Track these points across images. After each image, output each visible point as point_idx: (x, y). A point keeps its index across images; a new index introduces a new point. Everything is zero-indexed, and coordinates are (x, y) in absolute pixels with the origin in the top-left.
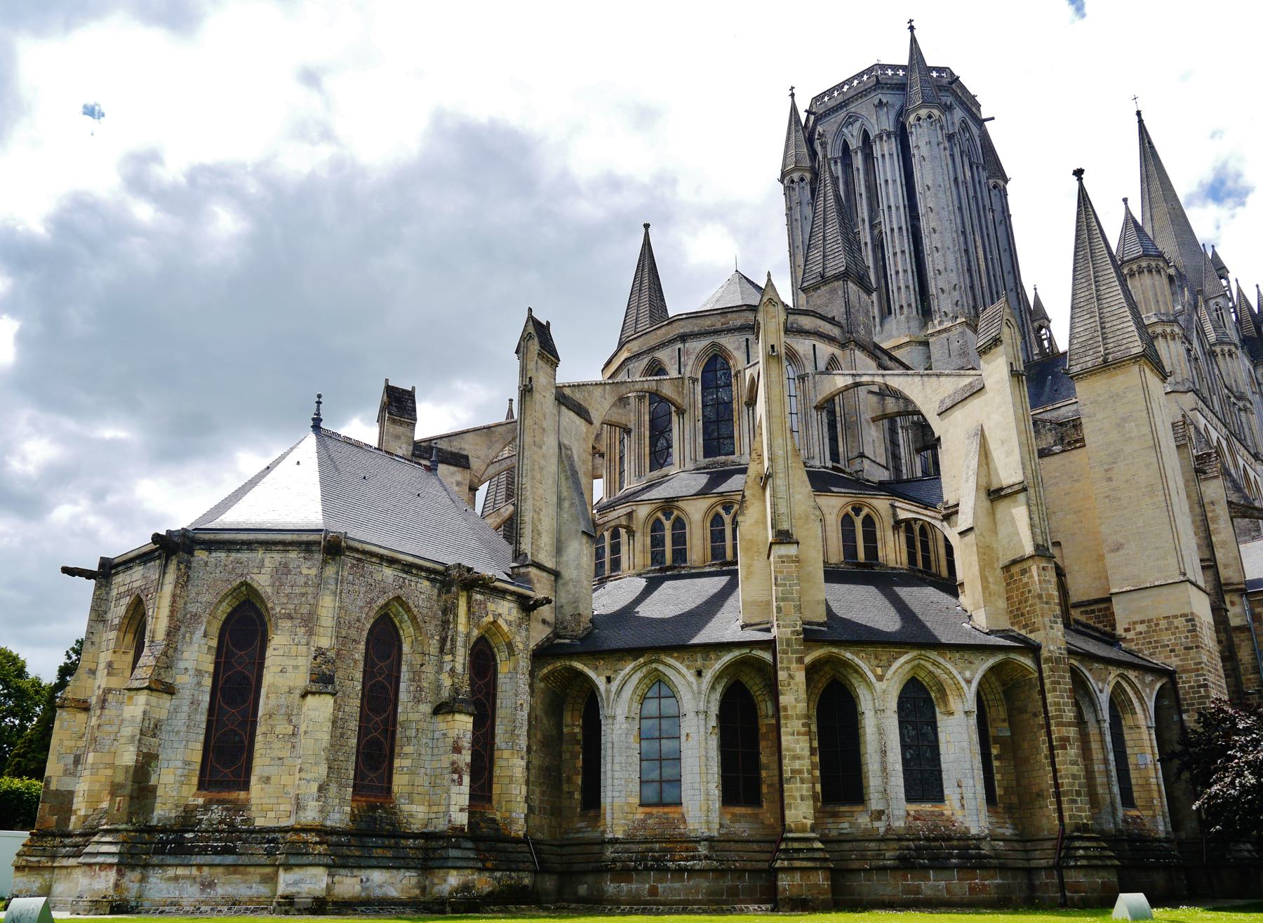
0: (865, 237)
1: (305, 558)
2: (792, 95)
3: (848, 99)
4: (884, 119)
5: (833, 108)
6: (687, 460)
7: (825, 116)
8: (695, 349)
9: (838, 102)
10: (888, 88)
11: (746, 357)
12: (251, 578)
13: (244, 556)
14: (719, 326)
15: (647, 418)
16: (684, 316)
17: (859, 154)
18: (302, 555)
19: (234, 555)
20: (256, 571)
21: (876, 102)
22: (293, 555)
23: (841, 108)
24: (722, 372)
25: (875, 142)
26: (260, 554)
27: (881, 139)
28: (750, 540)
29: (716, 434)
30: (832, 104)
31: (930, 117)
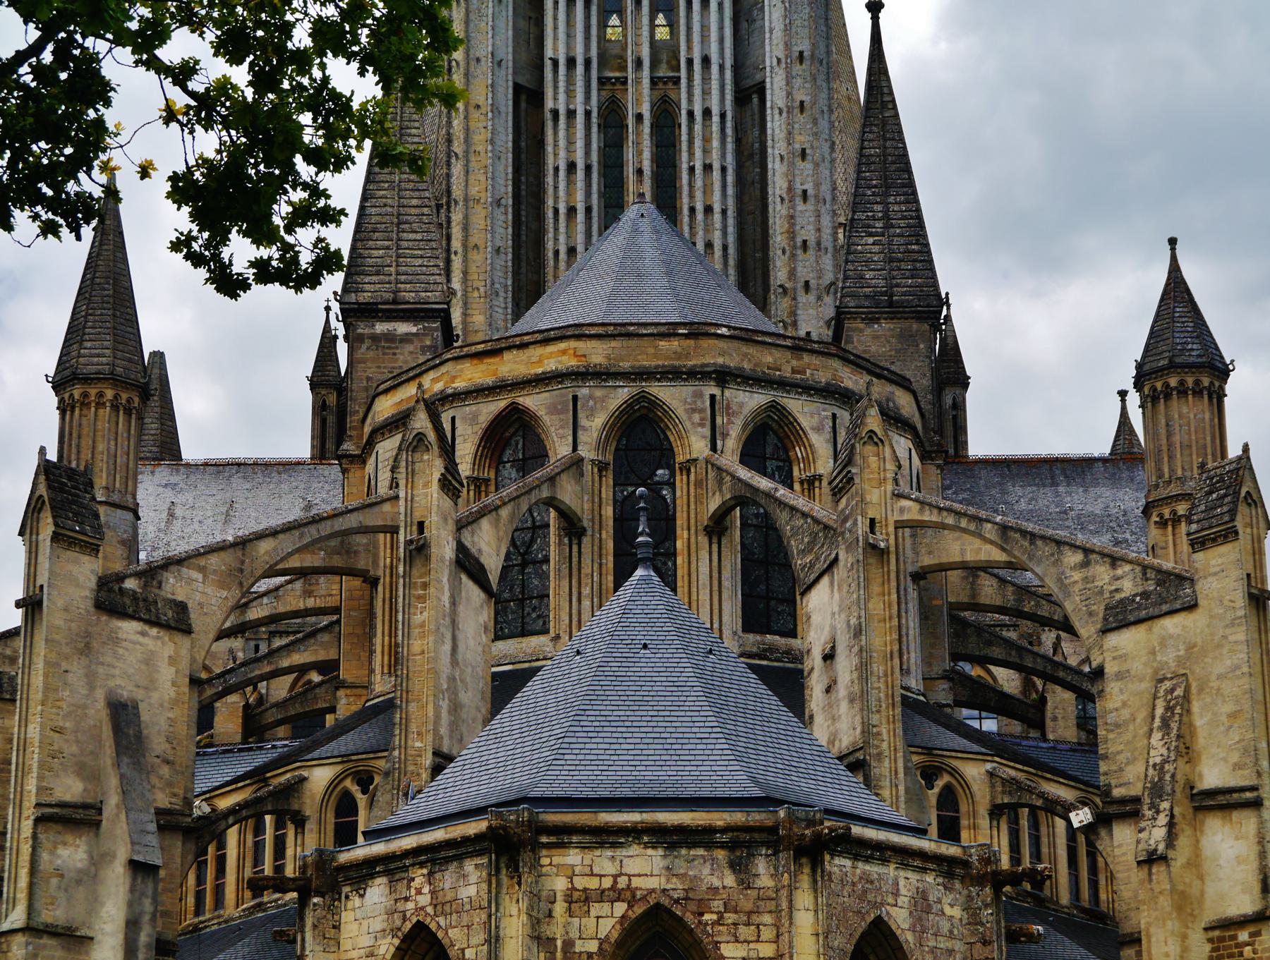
0: (638, 102)
1: (946, 888)
6: (727, 633)
8: (741, 405)
12: (888, 913)
13: (874, 869)
14: (787, 373)
15: (609, 511)
16: (724, 331)
18: (940, 880)
19: (860, 864)
20: (890, 900)
22: (930, 878)
26: (891, 871)
28: (1183, 892)
29: (763, 587)
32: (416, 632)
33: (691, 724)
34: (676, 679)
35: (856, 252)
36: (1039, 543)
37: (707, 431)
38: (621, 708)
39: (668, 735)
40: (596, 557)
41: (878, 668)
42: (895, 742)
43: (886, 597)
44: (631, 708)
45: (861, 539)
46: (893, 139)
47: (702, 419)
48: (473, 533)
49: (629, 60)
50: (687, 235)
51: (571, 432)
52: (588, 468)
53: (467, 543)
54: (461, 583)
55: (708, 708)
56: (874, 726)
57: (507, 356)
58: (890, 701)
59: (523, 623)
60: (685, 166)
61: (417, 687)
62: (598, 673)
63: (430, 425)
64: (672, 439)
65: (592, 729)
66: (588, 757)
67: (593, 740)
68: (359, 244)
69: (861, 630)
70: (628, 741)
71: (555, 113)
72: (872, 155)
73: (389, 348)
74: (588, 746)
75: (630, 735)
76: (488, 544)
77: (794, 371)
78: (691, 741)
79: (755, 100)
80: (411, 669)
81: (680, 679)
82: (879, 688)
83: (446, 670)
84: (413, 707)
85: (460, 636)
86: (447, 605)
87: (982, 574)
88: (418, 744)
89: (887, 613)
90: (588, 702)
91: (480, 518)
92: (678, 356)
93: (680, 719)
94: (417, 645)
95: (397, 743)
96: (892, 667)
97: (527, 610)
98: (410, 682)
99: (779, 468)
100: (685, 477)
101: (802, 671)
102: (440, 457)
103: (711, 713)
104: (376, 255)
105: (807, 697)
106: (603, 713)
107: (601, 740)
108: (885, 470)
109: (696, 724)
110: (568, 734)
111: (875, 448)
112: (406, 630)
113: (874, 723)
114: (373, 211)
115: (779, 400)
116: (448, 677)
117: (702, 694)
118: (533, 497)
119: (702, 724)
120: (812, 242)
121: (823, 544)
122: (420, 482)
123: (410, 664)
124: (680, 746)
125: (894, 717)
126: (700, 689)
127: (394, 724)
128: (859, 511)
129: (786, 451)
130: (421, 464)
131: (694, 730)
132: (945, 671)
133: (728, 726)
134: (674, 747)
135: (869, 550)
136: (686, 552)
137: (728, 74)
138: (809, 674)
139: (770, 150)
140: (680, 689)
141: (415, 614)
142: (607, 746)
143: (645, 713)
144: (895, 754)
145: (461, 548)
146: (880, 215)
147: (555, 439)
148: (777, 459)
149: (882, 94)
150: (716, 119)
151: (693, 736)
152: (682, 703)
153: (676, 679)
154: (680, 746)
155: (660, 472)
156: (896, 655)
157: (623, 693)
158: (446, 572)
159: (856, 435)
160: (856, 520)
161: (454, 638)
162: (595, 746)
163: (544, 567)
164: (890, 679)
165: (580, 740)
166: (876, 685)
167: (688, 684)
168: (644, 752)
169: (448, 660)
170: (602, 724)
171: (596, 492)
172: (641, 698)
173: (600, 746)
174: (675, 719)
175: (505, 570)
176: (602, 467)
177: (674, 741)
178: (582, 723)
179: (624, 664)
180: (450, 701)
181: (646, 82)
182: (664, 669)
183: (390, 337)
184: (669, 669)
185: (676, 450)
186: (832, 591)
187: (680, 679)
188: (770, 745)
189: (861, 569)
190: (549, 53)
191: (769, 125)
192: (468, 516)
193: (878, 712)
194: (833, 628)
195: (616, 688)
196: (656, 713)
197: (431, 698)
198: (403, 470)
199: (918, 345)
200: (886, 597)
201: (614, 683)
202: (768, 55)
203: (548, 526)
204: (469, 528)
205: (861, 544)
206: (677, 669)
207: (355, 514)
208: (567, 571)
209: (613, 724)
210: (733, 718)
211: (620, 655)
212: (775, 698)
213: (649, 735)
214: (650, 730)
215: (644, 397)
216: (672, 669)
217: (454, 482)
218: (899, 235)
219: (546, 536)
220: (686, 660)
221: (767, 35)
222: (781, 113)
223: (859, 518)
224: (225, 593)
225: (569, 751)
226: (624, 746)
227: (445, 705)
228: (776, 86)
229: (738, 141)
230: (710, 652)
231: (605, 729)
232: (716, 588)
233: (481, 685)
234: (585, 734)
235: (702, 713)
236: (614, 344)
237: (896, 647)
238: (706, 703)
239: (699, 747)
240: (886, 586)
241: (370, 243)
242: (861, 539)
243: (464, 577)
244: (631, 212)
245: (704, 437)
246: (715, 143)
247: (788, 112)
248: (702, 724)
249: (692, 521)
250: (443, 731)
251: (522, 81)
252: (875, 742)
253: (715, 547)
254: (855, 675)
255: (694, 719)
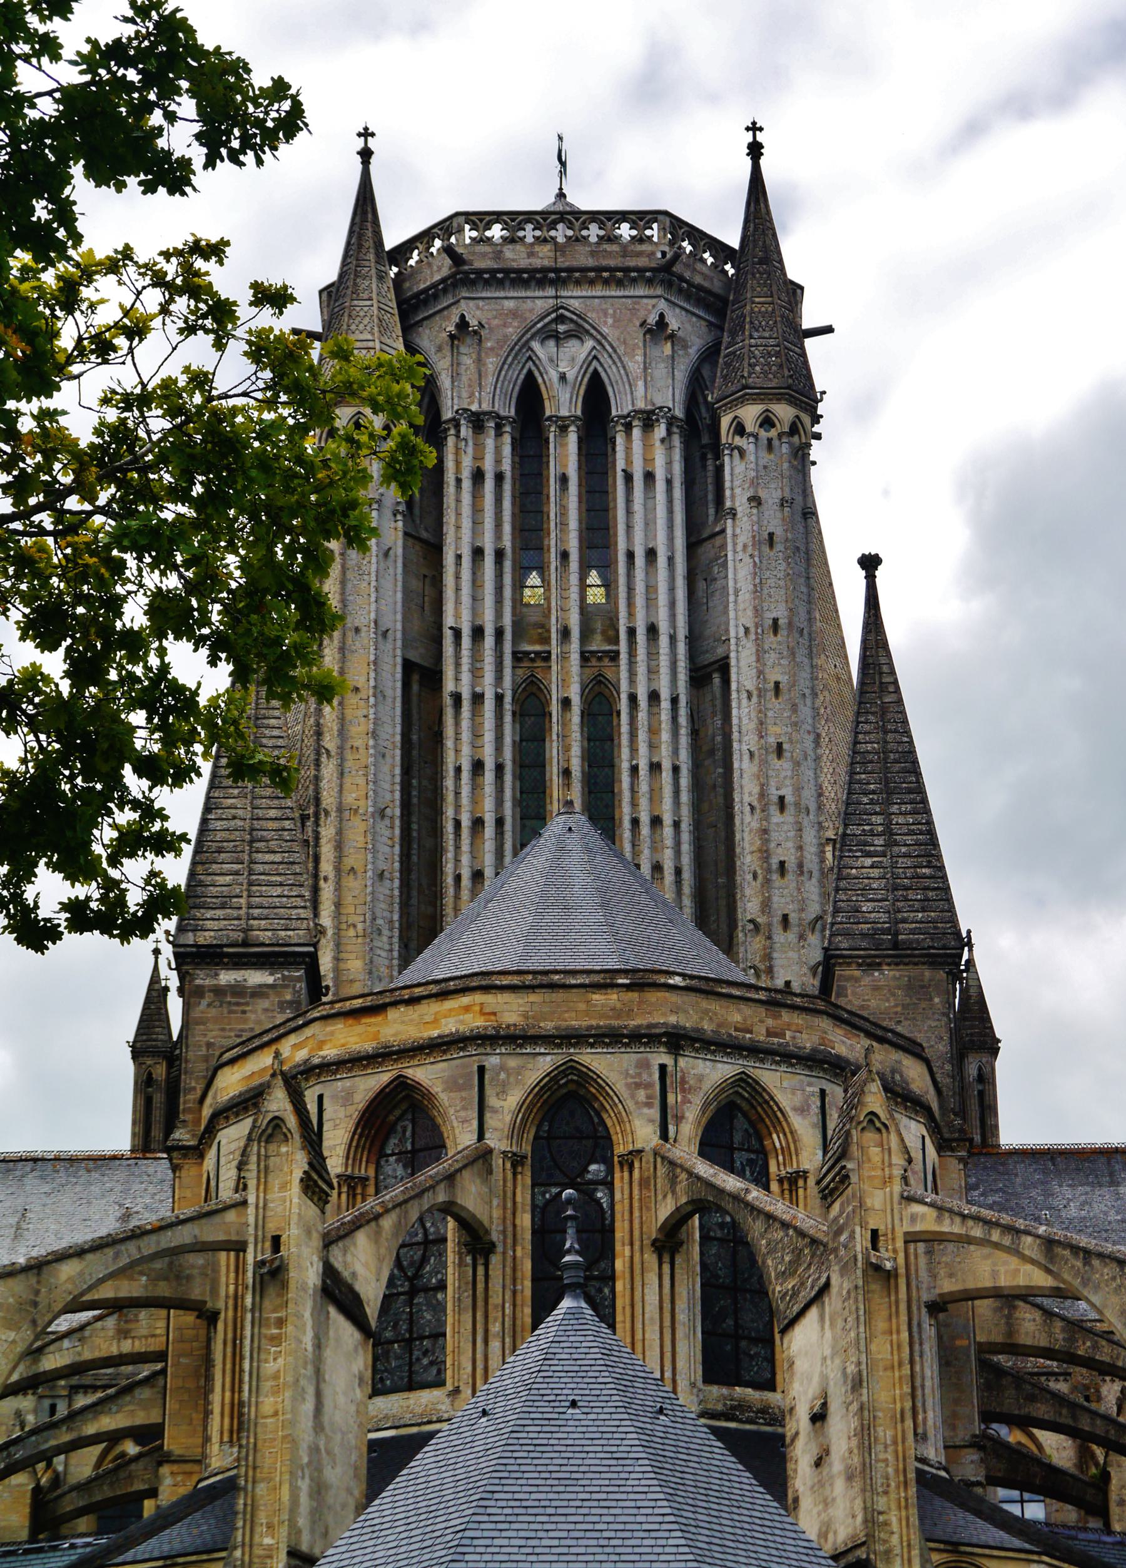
0: (564, 683)
2: (366, 154)
3: (570, 270)
4: (660, 371)
5: (520, 271)
6: (682, 1384)
7: (487, 283)
8: (700, 1078)
9: (537, 263)
10: (680, 291)
11: (820, 1136)
15: (525, 1220)
16: (677, 980)
17: (572, 438)
21: (653, 319)
23: (542, 283)
24: (745, 1155)
25: (628, 427)
27: (648, 425)
29: (730, 1322)
30: (516, 257)
31: (767, 422)
32: (267, 1385)
33: (635, 1511)
34: (614, 1449)
35: (848, 877)
36: (1096, 1262)
37: (655, 1113)
38: (541, 1489)
39: (604, 1527)
40: (508, 1282)
41: (884, 1432)
42: (908, 1535)
43: (895, 1337)
44: (555, 1489)
45: (860, 1257)
46: (896, 731)
47: (648, 1097)
48: (345, 1252)
49: (553, 630)
50: (628, 855)
51: (476, 1115)
52: (497, 1162)
53: (337, 1264)
54: (328, 1318)
55: (658, 1489)
56: (880, 1513)
57: (392, 1014)
58: (902, 1478)
59: (411, 1372)
60: (625, 766)
61: (268, 1462)
62: (510, 1441)
63: (289, 1107)
64: (609, 1123)
65: (502, 1518)
66: (497, 1557)
67: (504, 1534)
68: (199, 868)
69: (861, 1381)
70: (551, 1534)
71: (457, 698)
72: (868, 752)
73: (238, 1004)
74: (496, 1542)
75: (553, 1526)
76: (366, 1265)
77: (769, 1034)
78: (636, 1534)
79: (717, 680)
80: (260, 1436)
81: (621, 1449)
82: (886, 1460)
83: (306, 1437)
84: (261, 1489)
85: (327, 1392)
86: (310, 1348)
87: (1021, 1304)
88: (268, 1541)
89: (896, 1357)
90: (497, 1481)
91: (353, 1231)
92: (617, 1013)
93: (621, 1504)
94: (268, 1403)
95: (239, 1539)
96: (903, 1431)
97: (416, 1353)
98: (259, 1455)
99: (751, 1162)
100: (626, 1174)
101: (782, 1437)
102: (303, 1148)
103: (662, 1496)
104: (221, 882)
105: (790, 1473)
106: (517, 1496)
107: (514, 1534)
108: (890, 1165)
109: (643, 1511)
110: (470, 1526)
111: (877, 1136)
112: (254, 1383)
113: (880, 1509)
114: (219, 825)
115: (750, 1071)
116: (309, 1447)
117: (649, 1469)
118: (426, 1202)
119: (650, 1511)
120: (791, 865)
121: (810, 1265)
122: (275, 1182)
123: (259, 1430)
124: (619, 1542)
125: (907, 1500)
126: (647, 1462)
127: (236, 1513)
128: (857, 1220)
129: (761, 1140)
130: (278, 1159)
131: (639, 1519)
132: (974, 1436)
133: (685, 1514)
134: (613, 1542)
135: (870, 1272)
136: (627, 1275)
137: (682, 648)
138: (793, 1440)
139: (735, 745)
140: (621, 1462)
141: (266, 1361)
142: (522, 1542)
143: (573, 1496)
144: (909, 1552)
145: (329, 1271)
146: (880, 829)
147: (455, 1124)
148: (748, 1150)
149: (881, 673)
150: (665, 705)
151: (638, 1527)
152: (623, 1482)
153: (614, 1449)
154: (619, 1542)
155: (593, 1167)
156: (908, 1415)
157: (543, 1468)
158: (309, 1304)
159: (852, 1119)
160: (853, 1232)
161: (318, 1395)
162: (505, 1542)
163: (440, 1296)
164: (900, 1448)
165: (486, 1534)
166: (882, 1456)
167: (632, 1455)
168: (573, 1550)
169: (310, 1424)
170: (517, 1511)
171: (509, 1194)
172: (568, 1475)
173: (514, 1542)
174: (614, 1504)
175: (388, 1300)
176: (516, 1160)
177: (612, 1534)
178: (489, 1511)
179: (545, 1429)
180: (312, 1479)
181: (575, 658)
182: (598, 1435)
183: (238, 990)
184: (605, 1436)
185: (614, 1138)
186: (823, 1328)
187: (621, 1449)
188: (741, 1539)
189: (861, 1298)
190: (449, 620)
191: (734, 712)
192: (338, 1228)
193: (886, 1493)
194: (824, 1378)
195: (536, 1462)
196: (587, 1496)
197: (287, 1477)
198: (253, 1166)
199: (931, 999)
200: (895, 1337)
201: (532, 1455)
202: (732, 623)
203: (445, 1240)
204: (340, 1244)
205: (860, 1264)
206: (616, 1436)
207: (189, 1226)
208: (470, 1301)
209: (530, 1511)
210: (690, 1502)
211: (540, 1416)
212: (748, 1474)
213: (579, 1526)
214: (581, 1518)
215: (572, 1067)
216: (609, 1436)
217: (320, 1183)
218: (905, 856)
219: (442, 1254)
220: (628, 1423)
221: (732, 598)
222: (749, 697)
223: (858, 1229)
224: (12, 1335)
225: (471, 1549)
226: (545, 1542)
227: (304, 1485)
228: (742, 663)
229: (694, 733)
230: (661, 1411)
231: (521, 1518)
232: (667, 1323)
233: (353, 1458)
234: (492, 1526)
235: (650, 1496)
236: (533, 997)
237: (908, 1405)
238: (655, 1482)
239: (646, 1542)
240: (894, 1321)
241: (214, 866)
242: (860, 1257)
243: (332, 1311)
244: (556, 826)
245: (651, 1121)
246: (665, 736)
247: (759, 696)
248: (650, 1511)
249: (636, 1234)
250: (302, 1522)
251: (414, 656)
252: (882, 1535)
253: (666, 1268)
254: (854, 1442)
255: (639, 1504)
